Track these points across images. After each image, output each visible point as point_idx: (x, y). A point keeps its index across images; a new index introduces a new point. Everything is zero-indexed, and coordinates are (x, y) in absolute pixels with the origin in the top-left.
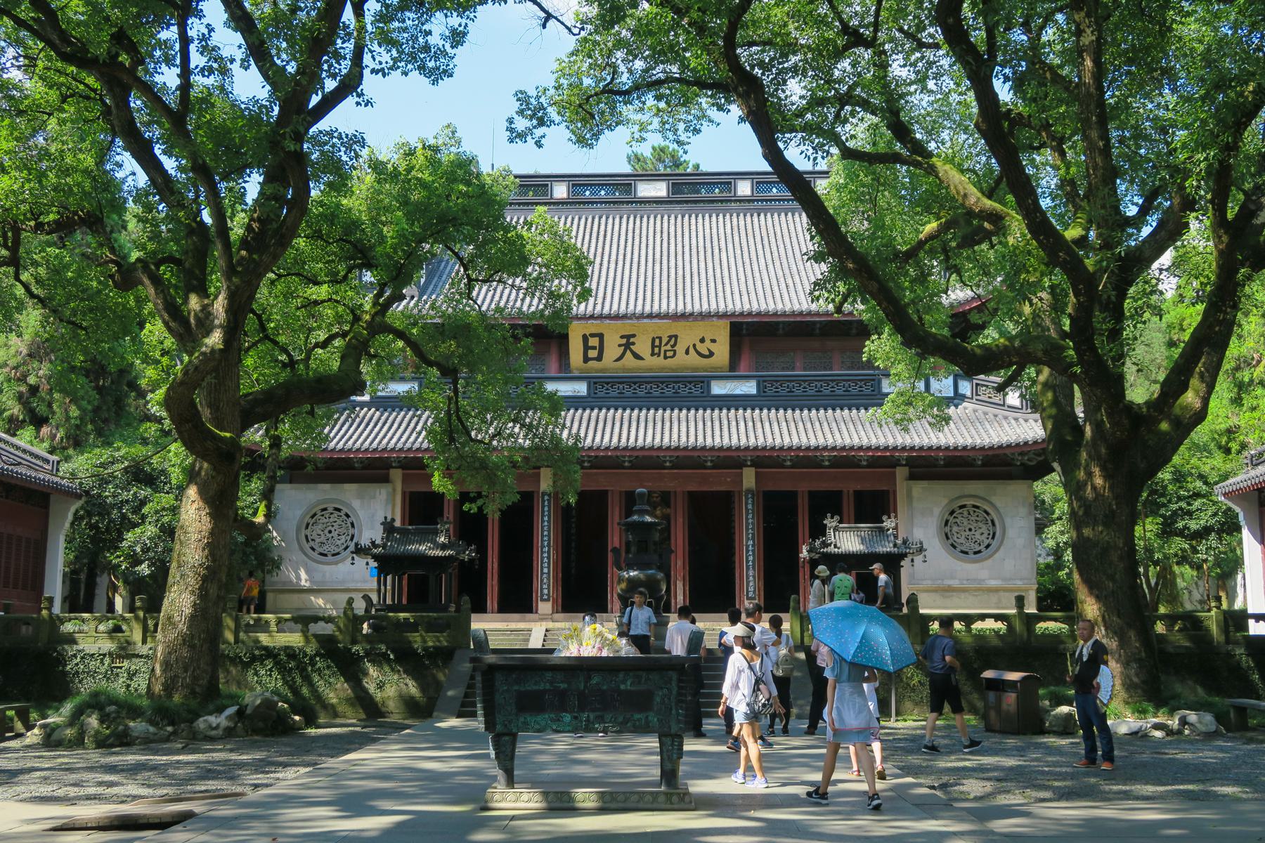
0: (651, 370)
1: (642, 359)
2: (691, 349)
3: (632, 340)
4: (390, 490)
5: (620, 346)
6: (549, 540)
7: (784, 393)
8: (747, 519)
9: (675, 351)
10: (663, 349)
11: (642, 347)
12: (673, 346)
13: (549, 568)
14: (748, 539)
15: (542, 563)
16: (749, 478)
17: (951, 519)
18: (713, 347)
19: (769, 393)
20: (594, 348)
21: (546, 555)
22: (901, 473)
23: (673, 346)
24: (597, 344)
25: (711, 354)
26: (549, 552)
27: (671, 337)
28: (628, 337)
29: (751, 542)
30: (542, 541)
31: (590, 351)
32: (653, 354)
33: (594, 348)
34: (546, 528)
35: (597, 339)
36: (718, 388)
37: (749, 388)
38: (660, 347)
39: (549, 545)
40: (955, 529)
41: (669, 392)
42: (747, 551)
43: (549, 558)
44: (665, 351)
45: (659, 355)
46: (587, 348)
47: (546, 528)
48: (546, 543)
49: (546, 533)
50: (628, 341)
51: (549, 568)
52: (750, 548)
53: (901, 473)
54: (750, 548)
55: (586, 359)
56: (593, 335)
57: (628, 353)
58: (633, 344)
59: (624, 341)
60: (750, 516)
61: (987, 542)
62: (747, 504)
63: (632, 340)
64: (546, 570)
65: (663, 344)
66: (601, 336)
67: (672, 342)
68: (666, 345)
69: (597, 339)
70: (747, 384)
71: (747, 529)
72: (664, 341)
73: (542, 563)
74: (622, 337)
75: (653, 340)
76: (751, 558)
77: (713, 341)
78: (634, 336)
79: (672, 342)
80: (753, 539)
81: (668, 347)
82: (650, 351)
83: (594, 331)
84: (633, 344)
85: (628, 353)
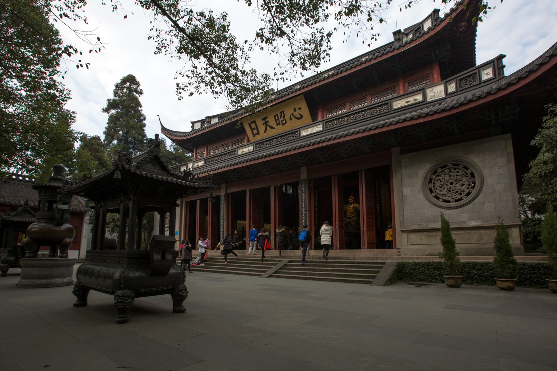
5: (263, 124)
9: (285, 120)
10: (280, 120)
12: (284, 118)
17: (434, 177)
18: (301, 112)
20: (254, 129)
24: (255, 127)
25: (302, 117)
27: (281, 113)
31: (254, 131)
32: (277, 125)
33: (254, 129)
38: (278, 119)
40: (438, 184)
46: (252, 129)
55: (254, 135)
56: (252, 123)
57: (267, 126)
58: (268, 122)
59: (264, 122)
61: (467, 191)
62: (302, 187)
66: (254, 122)
68: (281, 118)
74: (263, 120)
75: (275, 117)
77: (300, 109)
78: (266, 118)
79: (283, 115)
81: (282, 119)
82: (276, 124)
84: (268, 122)
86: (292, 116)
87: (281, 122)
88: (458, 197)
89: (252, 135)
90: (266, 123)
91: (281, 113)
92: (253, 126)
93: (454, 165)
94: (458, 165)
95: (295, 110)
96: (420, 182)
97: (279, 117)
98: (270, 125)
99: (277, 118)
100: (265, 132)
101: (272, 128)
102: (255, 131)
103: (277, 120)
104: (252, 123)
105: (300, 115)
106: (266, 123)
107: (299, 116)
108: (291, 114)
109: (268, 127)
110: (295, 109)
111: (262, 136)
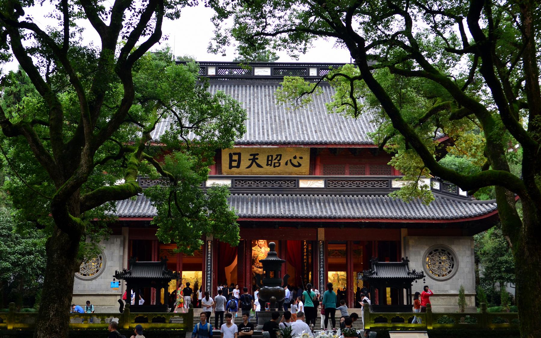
0: (266, 174)
1: (262, 167)
2: (289, 163)
3: (256, 157)
4: (122, 239)
5: (249, 160)
6: (211, 267)
7: (339, 187)
8: (320, 256)
9: (280, 163)
10: (273, 162)
11: (262, 160)
12: (279, 161)
13: (211, 283)
14: (320, 268)
15: (207, 280)
16: (321, 234)
18: (301, 161)
19: (331, 187)
20: (235, 161)
21: (209, 276)
22: (404, 232)
23: (279, 161)
25: (300, 165)
26: (211, 274)
27: (277, 156)
28: (254, 155)
29: (322, 269)
30: (207, 268)
32: (268, 165)
33: (235, 161)
34: (209, 261)
35: (237, 156)
36: (303, 184)
37: (320, 184)
38: (271, 161)
39: (211, 270)
41: (276, 185)
42: (320, 274)
43: (211, 277)
44: (275, 163)
45: (271, 165)
46: (231, 160)
47: (209, 261)
48: (209, 269)
49: (209, 263)
50: (254, 157)
51: (211, 283)
52: (322, 272)
53: (404, 232)
54: (322, 272)
55: (231, 167)
56: (235, 154)
58: (257, 159)
59: (252, 157)
60: (322, 255)
61: (449, 270)
63: (256, 157)
64: (209, 284)
65: (273, 159)
66: (239, 155)
67: (278, 158)
68: (275, 159)
69: (237, 156)
70: (319, 182)
71: (320, 262)
72: (274, 157)
73: (207, 280)
74: (251, 155)
75: (268, 157)
76: (322, 278)
77: (301, 158)
78: (258, 154)
79: (278, 158)
80: (323, 267)
81: (276, 161)
82: (266, 164)
83: (235, 152)
85: (254, 164)
86: (289, 161)
87: (273, 163)
88: (444, 273)
89: (228, 166)
90: (254, 160)
91: (277, 156)
92: (235, 157)
93: (442, 250)
94: (444, 251)
95: (295, 158)
96: (422, 259)
97: (274, 158)
98: (258, 163)
99: (270, 158)
100: (247, 168)
101: (259, 166)
102: (234, 164)
103: (270, 160)
104: (235, 154)
105: (298, 162)
106: (254, 160)
107: (297, 164)
108: (289, 159)
109: (254, 164)
110: (296, 156)
111: (243, 170)
